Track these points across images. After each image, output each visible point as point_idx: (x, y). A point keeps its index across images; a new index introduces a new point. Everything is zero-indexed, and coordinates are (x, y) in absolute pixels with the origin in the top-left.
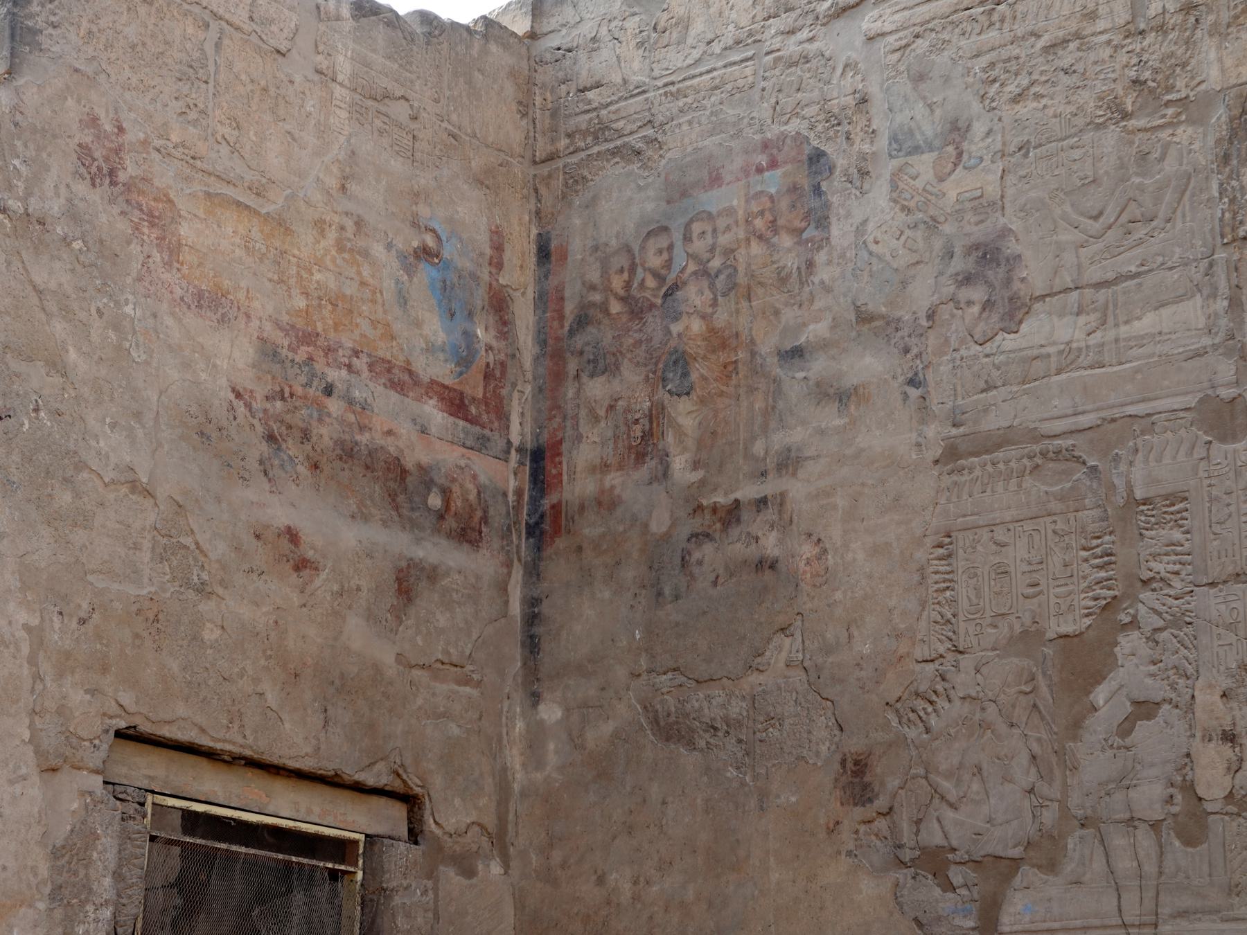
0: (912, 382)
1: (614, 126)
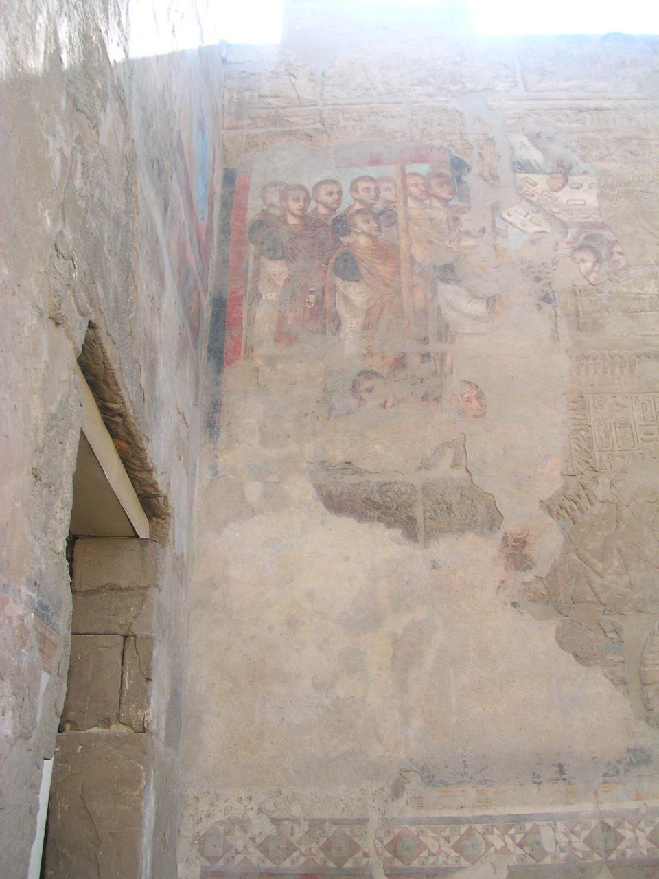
0: (546, 299)
1: (291, 119)
